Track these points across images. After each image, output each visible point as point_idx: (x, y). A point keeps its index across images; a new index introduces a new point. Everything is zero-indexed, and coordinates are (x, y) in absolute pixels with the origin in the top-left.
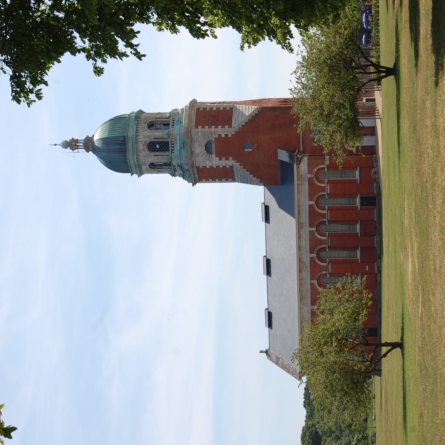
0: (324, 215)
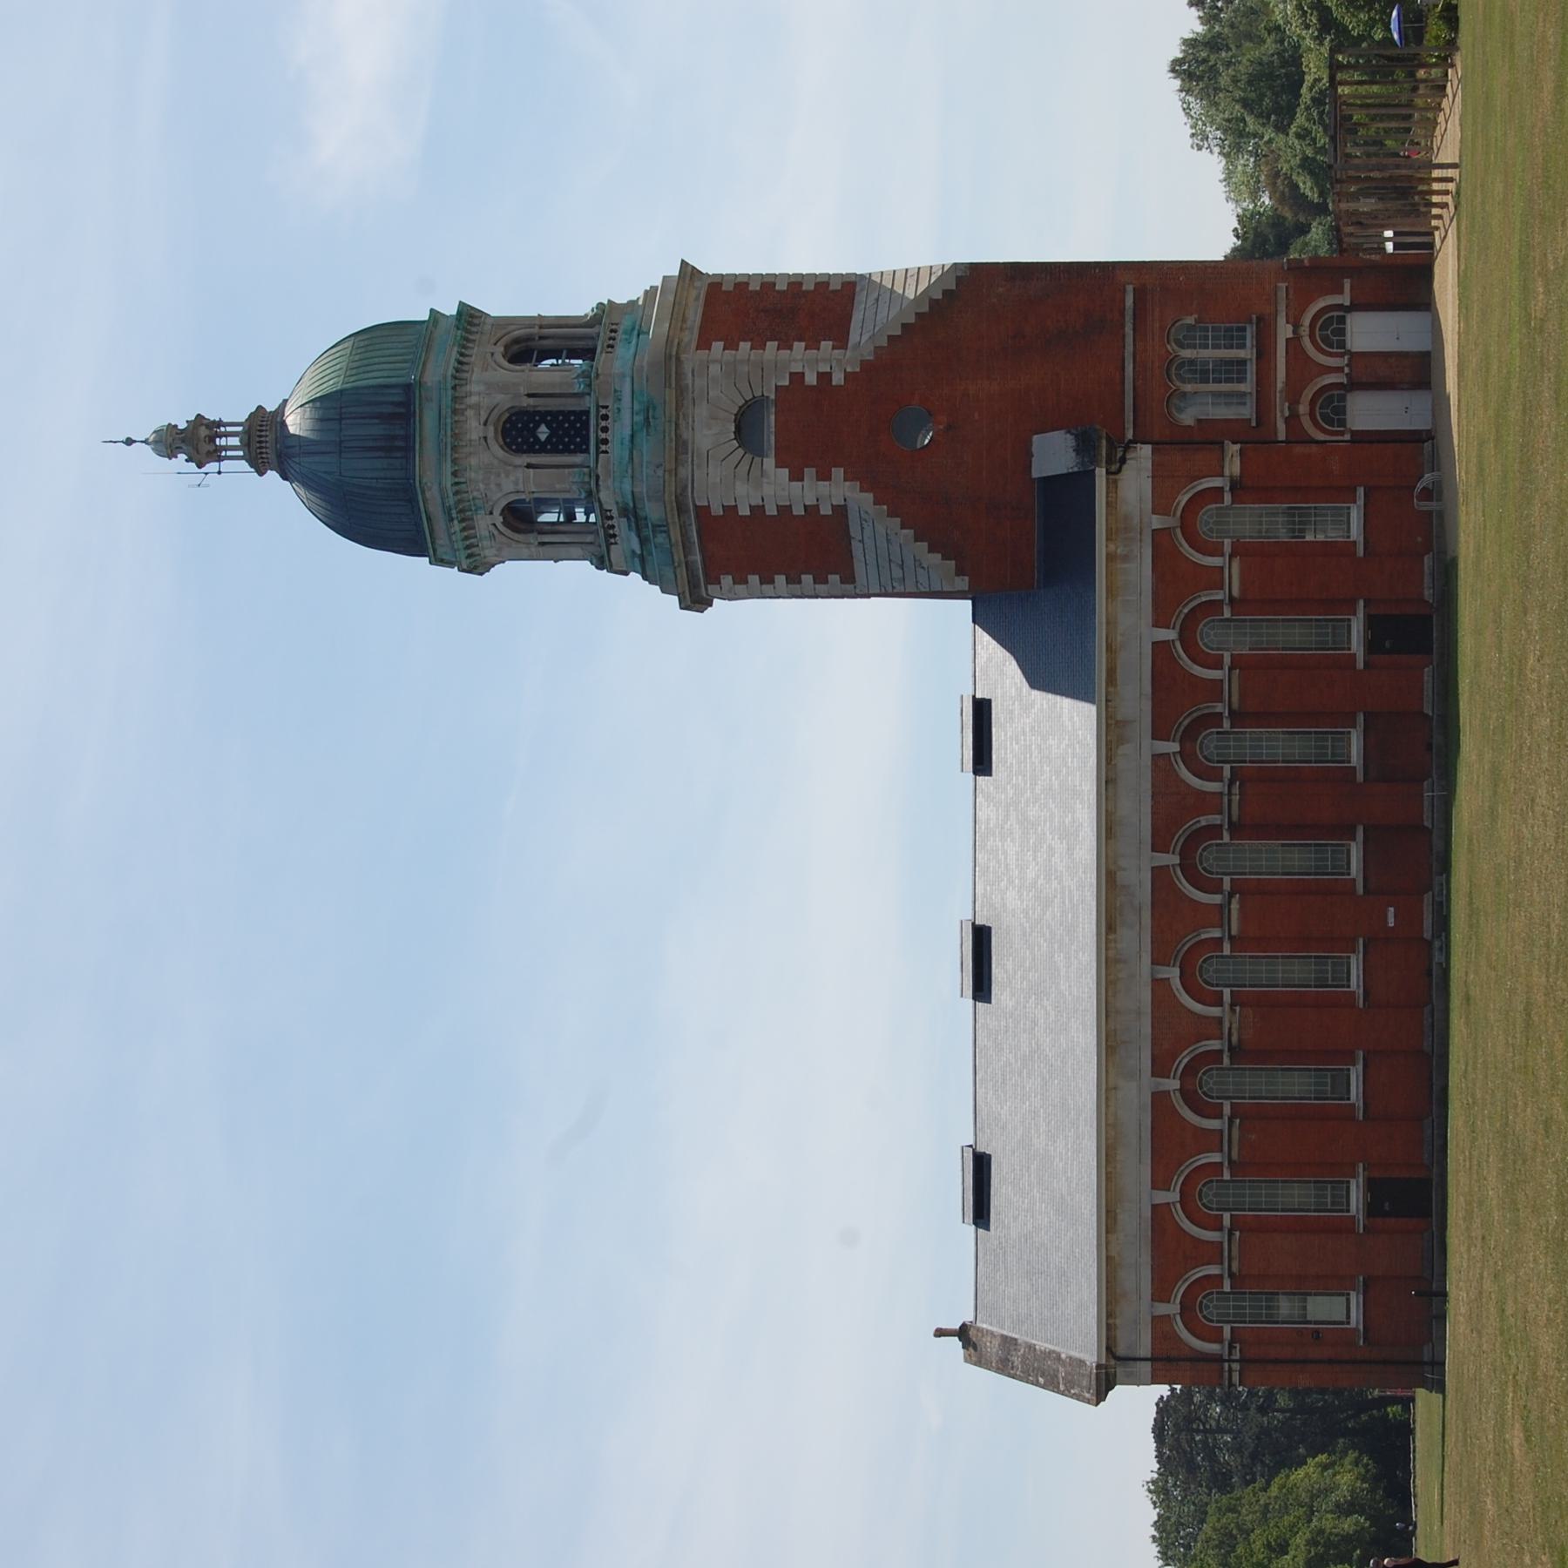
0: (1214, 690)
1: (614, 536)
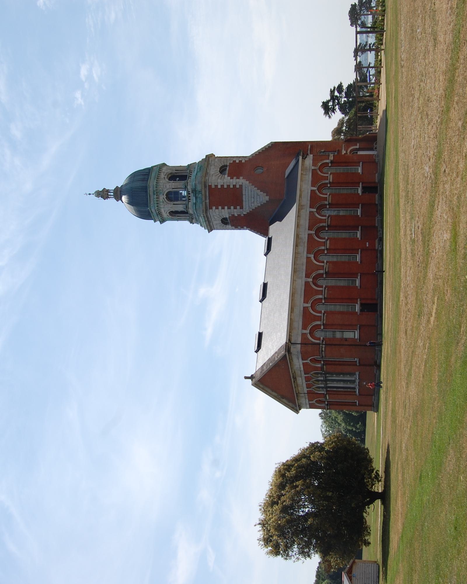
0: (325, 199)
1: (190, 199)
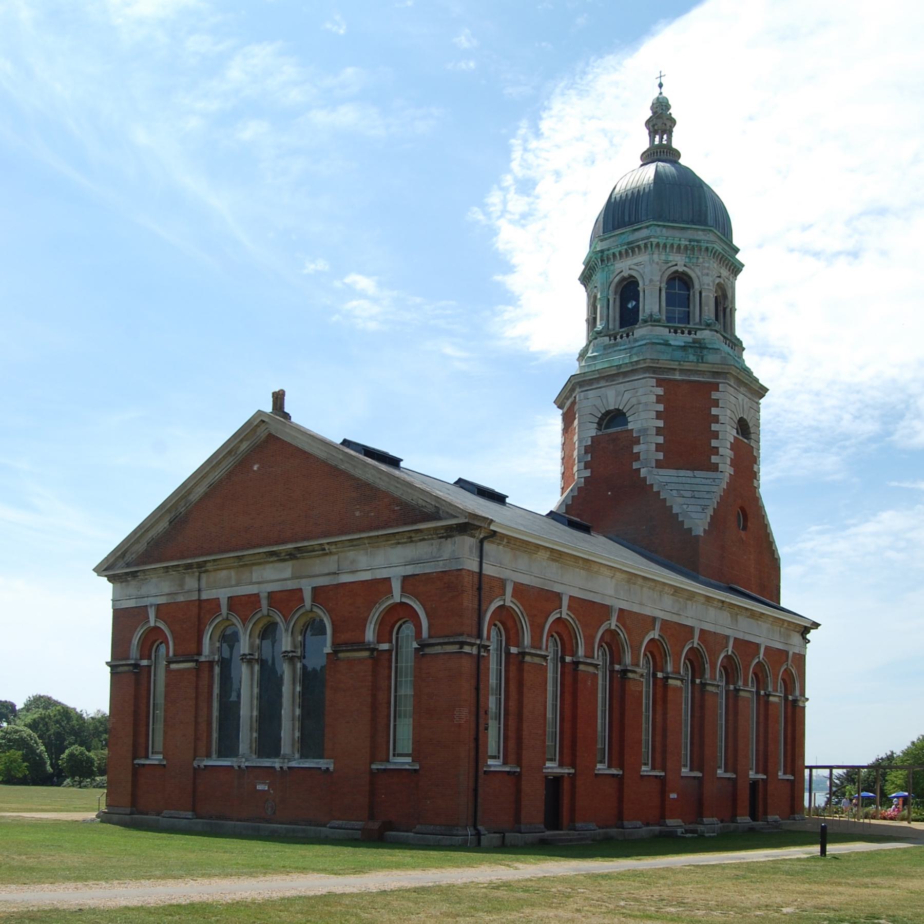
1: (676, 332)
